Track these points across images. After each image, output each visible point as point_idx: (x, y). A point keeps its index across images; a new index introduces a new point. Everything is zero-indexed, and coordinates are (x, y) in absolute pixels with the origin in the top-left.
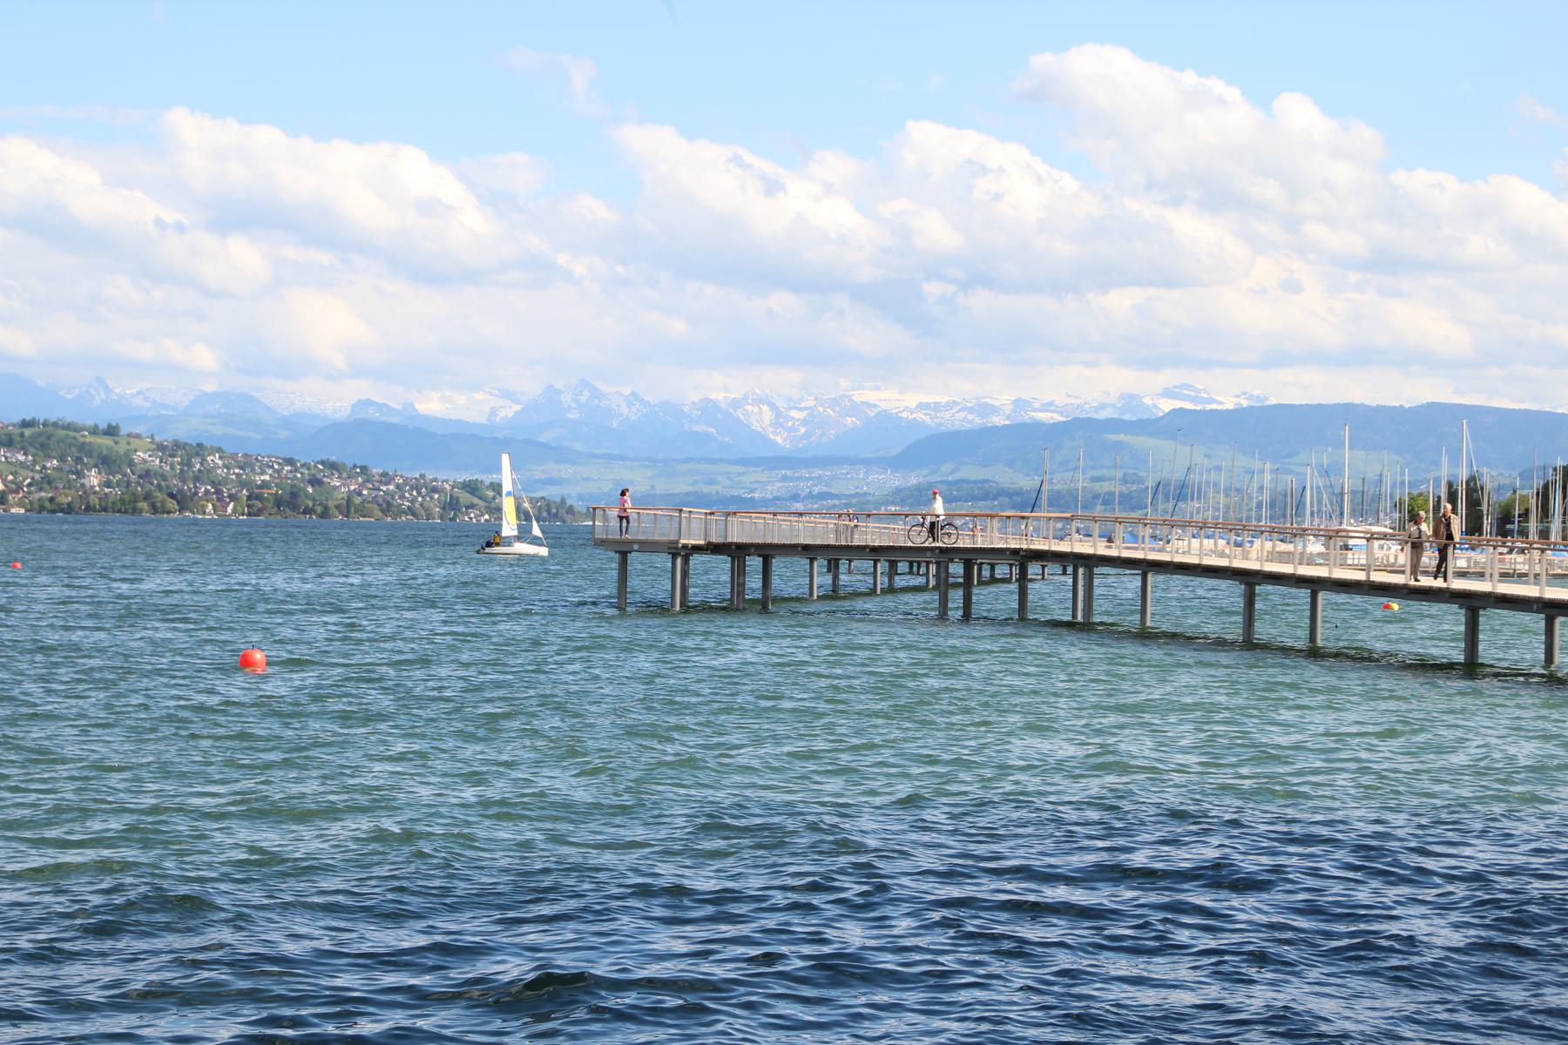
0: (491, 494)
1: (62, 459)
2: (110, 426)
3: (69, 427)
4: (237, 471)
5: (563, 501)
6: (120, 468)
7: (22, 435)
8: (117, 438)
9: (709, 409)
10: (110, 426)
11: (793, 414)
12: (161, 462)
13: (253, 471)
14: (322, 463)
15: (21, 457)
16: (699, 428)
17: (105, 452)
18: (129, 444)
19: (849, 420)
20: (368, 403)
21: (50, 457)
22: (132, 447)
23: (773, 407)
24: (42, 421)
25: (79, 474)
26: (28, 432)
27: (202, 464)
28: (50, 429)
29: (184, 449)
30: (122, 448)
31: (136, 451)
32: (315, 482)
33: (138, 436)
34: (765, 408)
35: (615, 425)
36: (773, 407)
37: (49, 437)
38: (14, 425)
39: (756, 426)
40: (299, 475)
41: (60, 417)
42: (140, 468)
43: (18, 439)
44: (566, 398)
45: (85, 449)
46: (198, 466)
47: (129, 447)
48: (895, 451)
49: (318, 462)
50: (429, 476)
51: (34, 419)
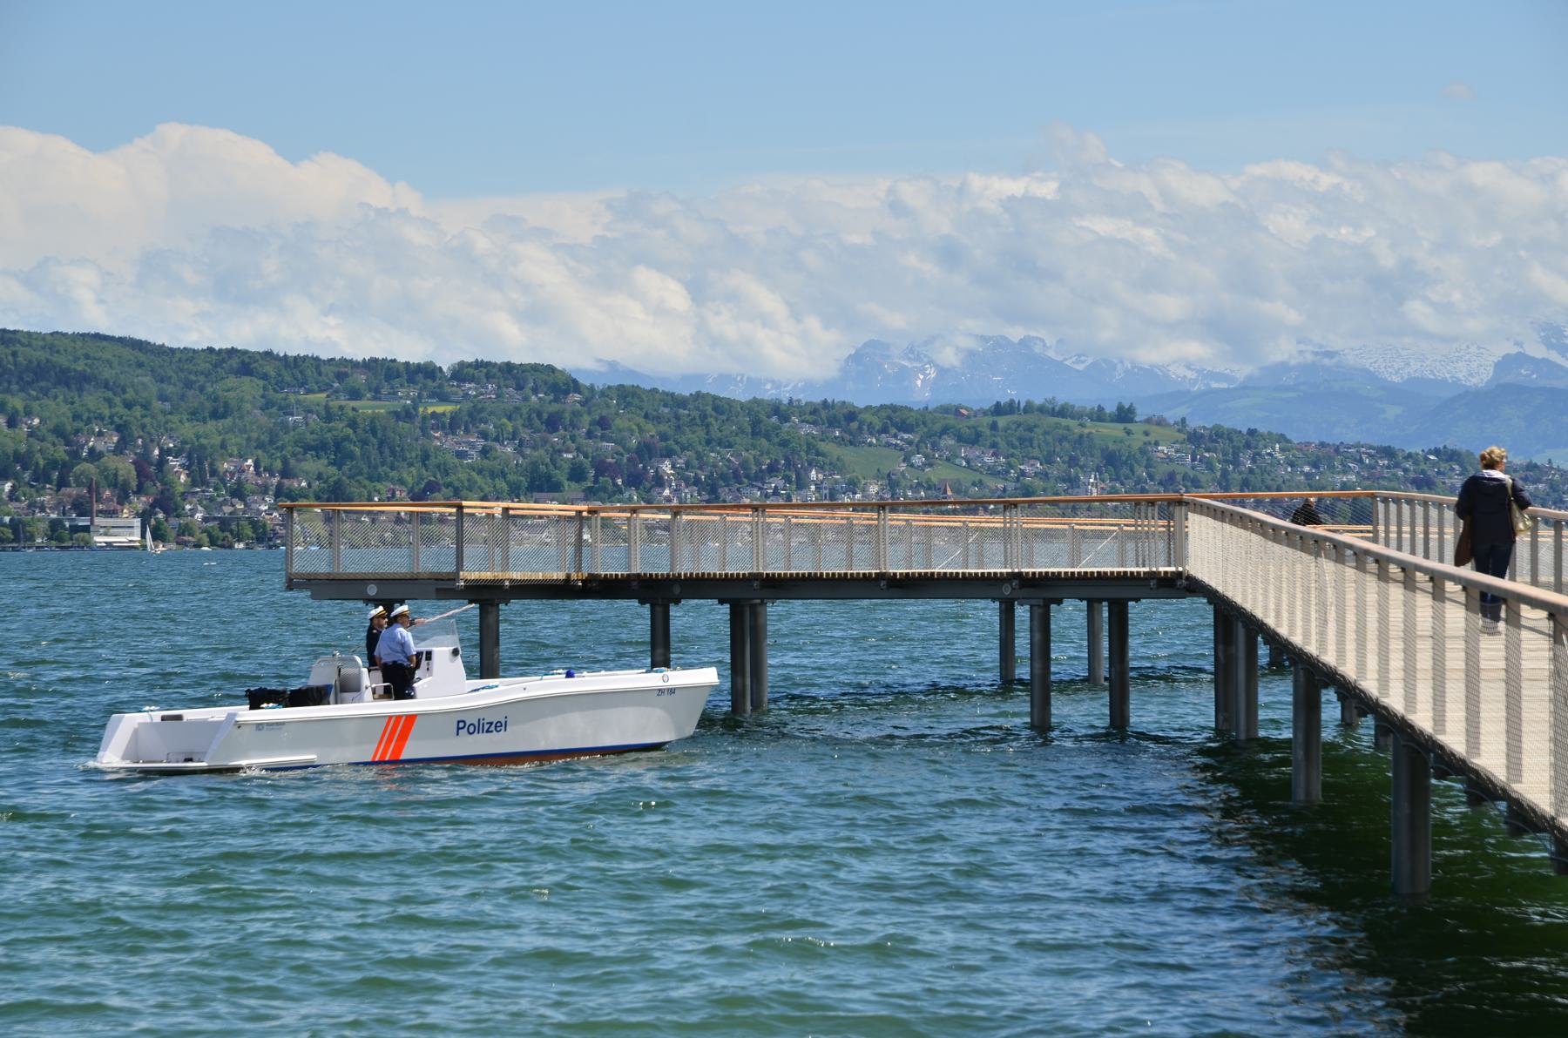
1: (1049, 460)
2: (1120, 408)
3: (1063, 412)
4: (1307, 469)
6: (1132, 470)
7: (994, 426)
8: (1129, 426)
10: (1120, 408)
12: (1193, 459)
13: (1332, 468)
14: (1437, 452)
15: (989, 460)
17: (1111, 447)
18: (1147, 434)
20: (1520, 359)
21: (1027, 458)
22: (1152, 439)
24: (1022, 407)
25: (1073, 482)
26: (1002, 421)
27: (1254, 461)
28: (1031, 419)
29: (1231, 440)
30: (1137, 441)
31: (1157, 444)
33: (1161, 422)
37: (1030, 429)
38: (985, 413)
40: (1401, 473)
41: (1050, 397)
42: (1162, 471)
43: (988, 432)
46: (1249, 464)
47: (1147, 439)
49: (1430, 452)
51: (1012, 401)
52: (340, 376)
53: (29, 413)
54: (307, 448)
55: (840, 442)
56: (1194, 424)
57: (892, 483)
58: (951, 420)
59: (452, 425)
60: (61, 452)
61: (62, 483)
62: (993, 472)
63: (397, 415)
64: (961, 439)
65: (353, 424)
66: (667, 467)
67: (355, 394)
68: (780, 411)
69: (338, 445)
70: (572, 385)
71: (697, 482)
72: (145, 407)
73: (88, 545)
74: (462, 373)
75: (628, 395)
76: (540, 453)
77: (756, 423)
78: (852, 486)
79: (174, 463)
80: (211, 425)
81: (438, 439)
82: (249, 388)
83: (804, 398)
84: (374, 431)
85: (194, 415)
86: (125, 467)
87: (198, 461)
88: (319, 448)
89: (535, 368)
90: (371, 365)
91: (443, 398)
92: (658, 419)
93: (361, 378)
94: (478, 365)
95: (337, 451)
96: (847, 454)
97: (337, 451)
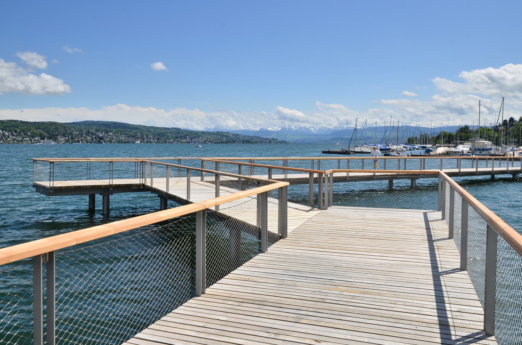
0: (276, 140)
3: (223, 132)
5: (285, 141)
9: (305, 127)
11: (317, 129)
16: (305, 131)
19: (324, 129)
23: (314, 128)
26: (217, 133)
32: (252, 139)
33: (231, 133)
34: (313, 128)
35: (293, 130)
36: (314, 128)
39: (312, 130)
44: (287, 127)
45: (224, 135)
48: (330, 133)
50: (268, 138)
52: (161, 129)
53: (133, 132)
54: (157, 135)
55: (203, 135)
56: (233, 133)
57: (207, 138)
58: (213, 133)
59: (170, 133)
60: (135, 135)
61: (135, 138)
62: (216, 137)
63: (165, 132)
64: (213, 135)
65: (161, 133)
66: (188, 137)
67: (162, 130)
68: (198, 132)
69: (160, 134)
70: (181, 130)
71: (190, 138)
72: (143, 131)
73: (135, 143)
74: (171, 128)
75: (185, 130)
76: (177, 135)
77: (196, 133)
78: (204, 138)
79: (145, 136)
80: (149, 133)
81: (168, 134)
82: (153, 129)
83: (201, 131)
84: (162, 133)
85: (148, 132)
86: (140, 136)
87: (147, 135)
88: (158, 135)
89: (178, 128)
90: (164, 128)
91: (170, 131)
92: (187, 133)
93: (163, 129)
94: (173, 128)
95: (159, 135)
96: (203, 135)
97: (159, 135)
